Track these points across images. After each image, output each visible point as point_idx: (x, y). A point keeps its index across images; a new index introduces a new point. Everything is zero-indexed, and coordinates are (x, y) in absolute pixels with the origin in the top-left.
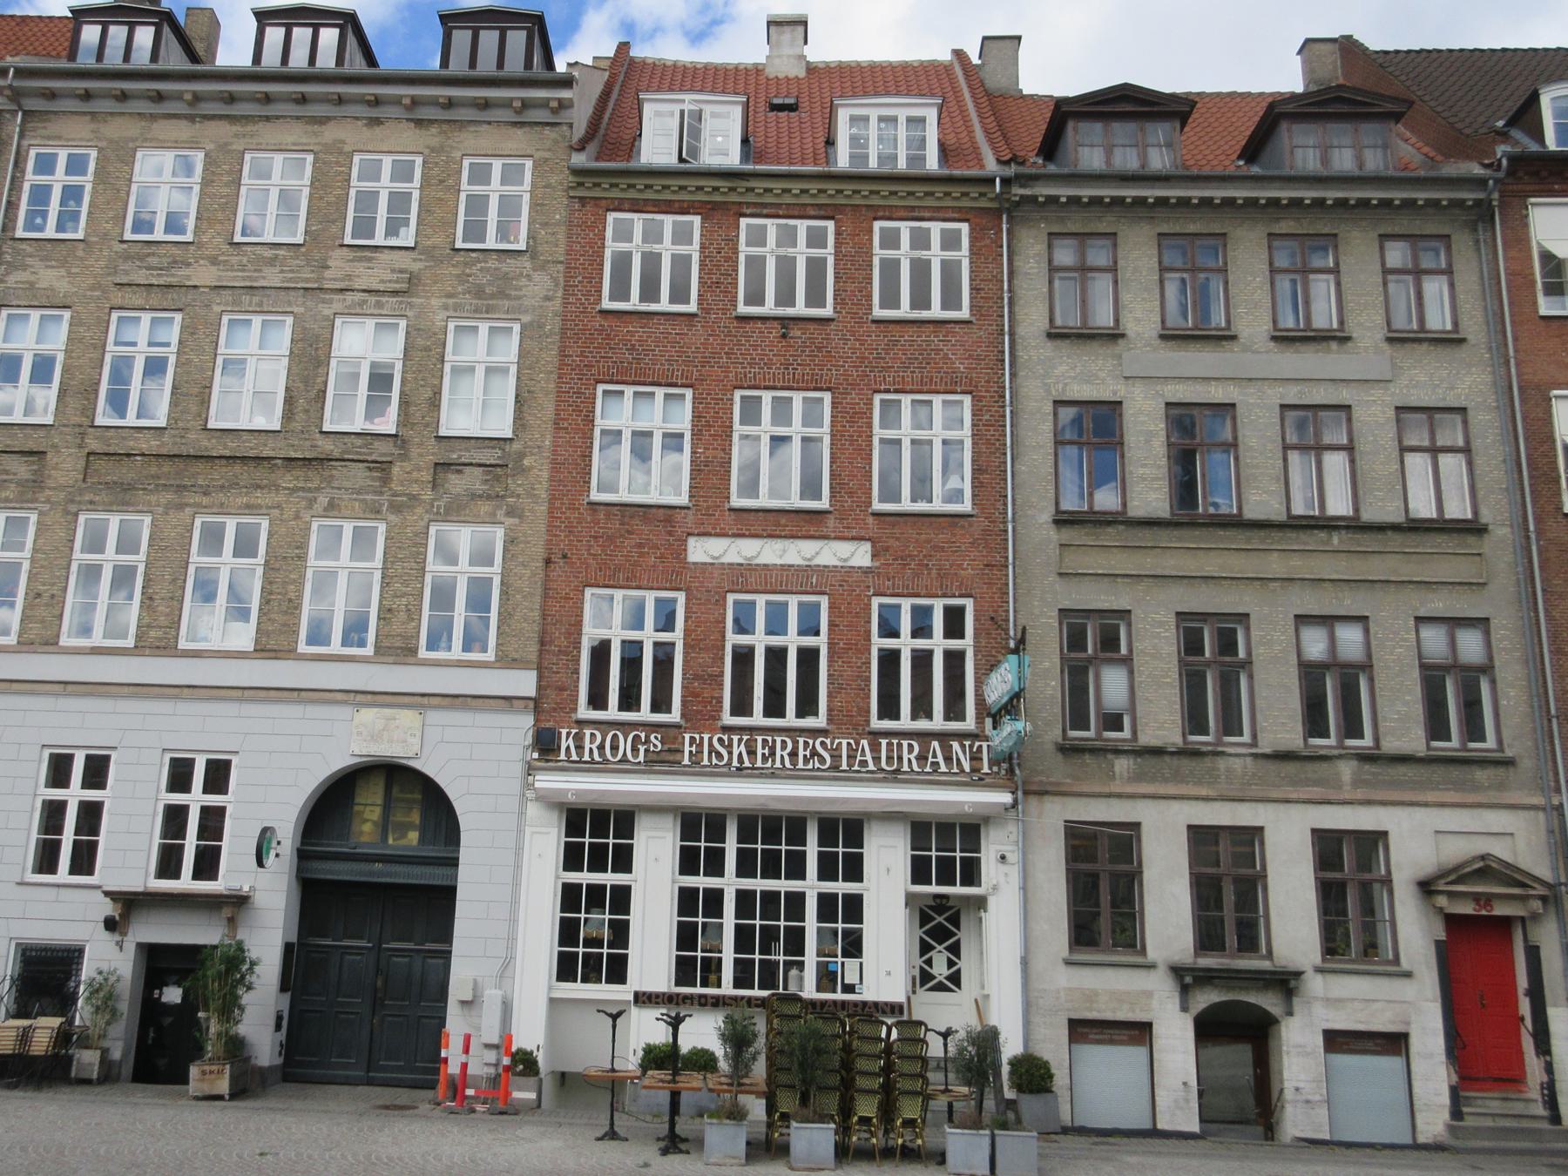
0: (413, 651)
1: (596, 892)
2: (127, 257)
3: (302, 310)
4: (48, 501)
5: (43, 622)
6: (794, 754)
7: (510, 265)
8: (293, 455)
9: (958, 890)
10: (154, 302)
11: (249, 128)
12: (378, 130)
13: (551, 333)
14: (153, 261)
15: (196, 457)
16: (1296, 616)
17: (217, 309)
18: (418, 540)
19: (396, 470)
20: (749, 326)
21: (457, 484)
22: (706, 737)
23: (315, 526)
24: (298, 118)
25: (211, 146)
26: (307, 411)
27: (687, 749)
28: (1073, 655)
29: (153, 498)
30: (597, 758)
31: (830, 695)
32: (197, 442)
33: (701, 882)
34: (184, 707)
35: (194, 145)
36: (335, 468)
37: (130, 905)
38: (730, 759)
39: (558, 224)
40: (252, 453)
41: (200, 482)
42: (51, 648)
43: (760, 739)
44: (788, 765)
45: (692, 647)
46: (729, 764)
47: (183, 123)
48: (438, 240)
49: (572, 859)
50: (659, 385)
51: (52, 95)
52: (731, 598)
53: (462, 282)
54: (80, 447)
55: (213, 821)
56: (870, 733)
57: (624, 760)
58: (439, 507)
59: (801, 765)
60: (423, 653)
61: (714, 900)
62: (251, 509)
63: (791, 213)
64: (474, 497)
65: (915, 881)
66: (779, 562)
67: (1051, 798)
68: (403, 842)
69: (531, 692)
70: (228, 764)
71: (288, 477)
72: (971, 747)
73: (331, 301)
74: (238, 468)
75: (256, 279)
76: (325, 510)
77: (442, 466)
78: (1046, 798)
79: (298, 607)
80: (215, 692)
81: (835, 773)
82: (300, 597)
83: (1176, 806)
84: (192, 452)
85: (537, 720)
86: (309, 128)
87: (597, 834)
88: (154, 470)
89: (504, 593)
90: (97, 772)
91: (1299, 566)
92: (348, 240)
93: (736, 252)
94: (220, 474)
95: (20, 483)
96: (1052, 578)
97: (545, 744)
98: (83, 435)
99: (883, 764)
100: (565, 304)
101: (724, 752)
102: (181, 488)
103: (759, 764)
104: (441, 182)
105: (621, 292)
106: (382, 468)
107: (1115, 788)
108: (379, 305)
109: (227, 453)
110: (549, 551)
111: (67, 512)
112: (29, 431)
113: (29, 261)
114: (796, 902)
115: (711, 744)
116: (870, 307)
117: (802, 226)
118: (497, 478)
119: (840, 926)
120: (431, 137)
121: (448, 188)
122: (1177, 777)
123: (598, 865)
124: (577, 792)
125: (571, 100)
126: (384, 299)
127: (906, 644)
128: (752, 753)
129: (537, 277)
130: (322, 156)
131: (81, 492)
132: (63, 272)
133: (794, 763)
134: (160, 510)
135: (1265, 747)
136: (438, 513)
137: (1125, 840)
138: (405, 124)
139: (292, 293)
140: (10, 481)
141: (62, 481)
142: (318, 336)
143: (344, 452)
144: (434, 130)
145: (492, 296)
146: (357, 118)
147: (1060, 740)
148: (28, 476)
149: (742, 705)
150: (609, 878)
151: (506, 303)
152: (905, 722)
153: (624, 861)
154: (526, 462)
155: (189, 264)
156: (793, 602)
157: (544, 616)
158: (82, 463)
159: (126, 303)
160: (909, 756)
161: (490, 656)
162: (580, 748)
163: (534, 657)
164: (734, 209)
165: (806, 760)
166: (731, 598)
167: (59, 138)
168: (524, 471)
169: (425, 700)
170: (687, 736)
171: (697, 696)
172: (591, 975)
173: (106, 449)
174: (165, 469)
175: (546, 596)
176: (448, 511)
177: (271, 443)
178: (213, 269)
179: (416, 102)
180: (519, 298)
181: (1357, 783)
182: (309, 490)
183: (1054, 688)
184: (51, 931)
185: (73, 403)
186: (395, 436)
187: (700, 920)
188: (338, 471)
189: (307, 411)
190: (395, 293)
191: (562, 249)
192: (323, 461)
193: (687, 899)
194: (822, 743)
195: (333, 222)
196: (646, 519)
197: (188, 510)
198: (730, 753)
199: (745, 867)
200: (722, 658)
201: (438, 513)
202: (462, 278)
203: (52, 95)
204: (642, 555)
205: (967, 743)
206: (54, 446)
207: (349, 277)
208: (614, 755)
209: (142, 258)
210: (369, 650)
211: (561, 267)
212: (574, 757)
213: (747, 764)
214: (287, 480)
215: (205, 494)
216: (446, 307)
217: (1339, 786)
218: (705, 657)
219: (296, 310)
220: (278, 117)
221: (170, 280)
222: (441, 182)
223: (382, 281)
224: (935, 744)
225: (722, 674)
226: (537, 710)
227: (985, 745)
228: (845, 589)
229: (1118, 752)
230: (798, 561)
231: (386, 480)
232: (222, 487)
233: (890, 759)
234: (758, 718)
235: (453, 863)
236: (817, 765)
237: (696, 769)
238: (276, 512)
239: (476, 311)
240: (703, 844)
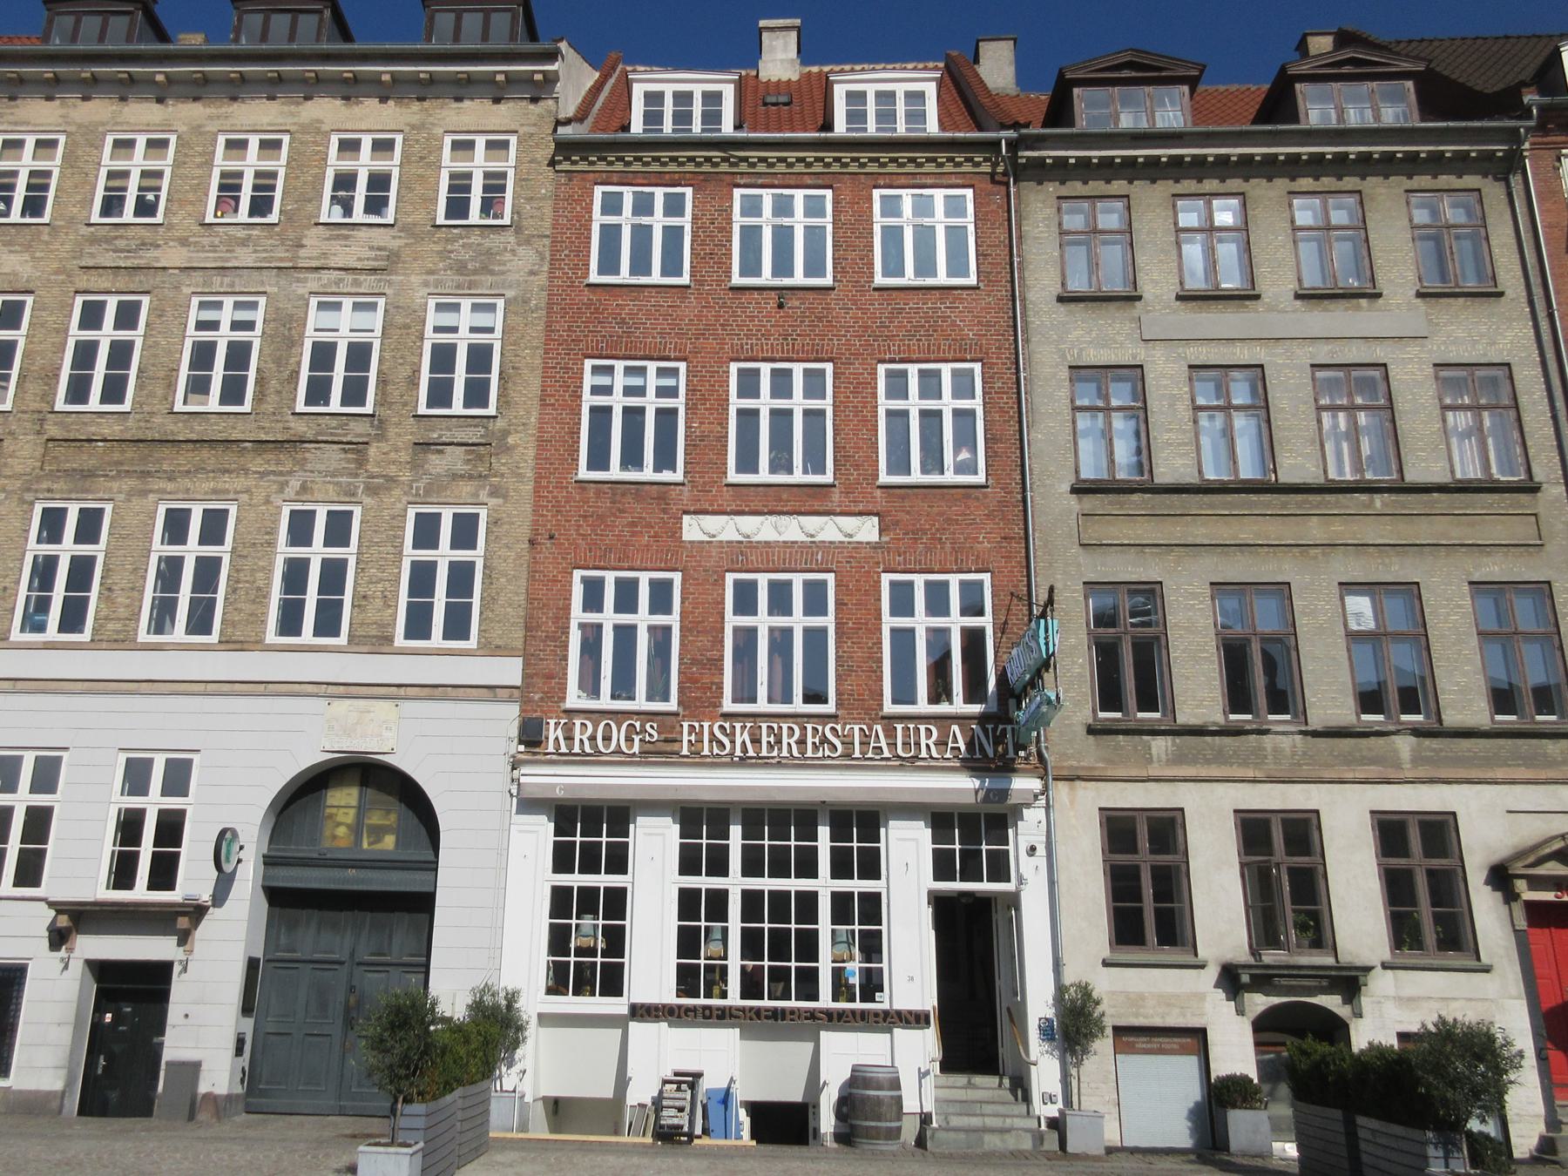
0: (389, 639)
1: (589, 895)
2: (93, 240)
6: (802, 742)
7: (495, 240)
8: (264, 437)
9: (985, 886)
10: (120, 285)
11: (223, 110)
13: (537, 308)
14: (121, 243)
16: (1340, 584)
17: (187, 290)
18: (395, 523)
19: (372, 451)
20: (745, 297)
21: (437, 464)
22: (706, 725)
25: (184, 128)
26: (279, 392)
27: (685, 738)
28: (1101, 630)
29: (115, 485)
30: (588, 750)
31: (838, 677)
32: (162, 426)
33: (704, 882)
36: (308, 450)
37: (76, 919)
38: (734, 748)
39: (543, 198)
41: (165, 467)
43: (764, 726)
44: (795, 753)
45: (690, 630)
46: (732, 754)
48: (419, 216)
49: (562, 861)
50: (651, 359)
52: (730, 578)
53: (443, 259)
54: (39, 433)
55: (171, 828)
56: (883, 718)
57: (618, 751)
58: (418, 489)
59: (809, 754)
60: (400, 641)
61: (718, 901)
62: (217, 493)
63: (787, 182)
64: (455, 477)
65: (938, 876)
66: (781, 539)
67: (1083, 784)
68: (378, 846)
69: (519, 683)
70: (188, 764)
71: (259, 460)
72: (995, 730)
73: (305, 280)
74: (205, 453)
75: (227, 260)
76: (297, 493)
77: (424, 446)
78: (1078, 783)
79: (267, 596)
81: (848, 761)
82: (269, 585)
83: (1220, 788)
84: (157, 436)
85: (522, 711)
86: (286, 108)
87: (589, 832)
88: (116, 456)
89: (487, 576)
91: (1339, 530)
93: (730, 221)
94: (185, 459)
96: (1076, 549)
97: (531, 736)
98: (42, 421)
99: (900, 751)
100: (551, 278)
101: (726, 741)
102: (145, 474)
103: (764, 753)
105: (609, 263)
106: (357, 449)
107: (1154, 771)
108: (356, 283)
109: (194, 437)
110: (535, 532)
111: (24, 502)
114: (808, 902)
115: (712, 733)
116: (872, 275)
117: (799, 195)
118: (480, 458)
119: (857, 927)
121: (429, 165)
122: (1220, 758)
123: (590, 866)
124: (566, 787)
125: (556, 72)
126: (362, 278)
127: (921, 622)
128: (756, 741)
129: (521, 251)
131: (39, 479)
132: (26, 257)
133: (803, 753)
134: (122, 497)
135: (1315, 722)
136: (417, 495)
137: (1167, 829)
139: (265, 272)
141: (19, 469)
142: (291, 316)
143: (318, 434)
145: (475, 272)
147: (1090, 721)
149: (746, 692)
150: (602, 880)
151: (490, 278)
152: (923, 706)
153: (618, 863)
154: (510, 440)
156: (798, 580)
157: (530, 599)
160: (928, 740)
161: (472, 643)
162: (569, 739)
163: (519, 644)
164: (728, 178)
165: (816, 747)
166: (730, 578)
167: (28, 124)
168: (508, 449)
169: (402, 691)
170: (686, 725)
171: (696, 681)
172: (583, 986)
173: (66, 435)
174: (129, 455)
175: (532, 578)
176: (428, 492)
177: (240, 426)
178: (184, 251)
180: (503, 273)
181: (1417, 760)
182: (281, 474)
183: (1081, 666)
185: (33, 388)
186: (373, 416)
187: (703, 924)
188: (312, 454)
189: (279, 392)
190: (374, 270)
191: (548, 223)
193: (688, 902)
194: (833, 729)
195: (310, 201)
196: (638, 497)
197: (152, 497)
198: (733, 742)
199: (751, 867)
200: (722, 641)
201: (417, 495)
202: (444, 255)
204: (634, 534)
205: (990, 727)
206: (11, 433)
207: (324, 255)
208: (607, 747)
209: (108, 240)
210: (342, 640)
211: (547, 242)
212: (564, 749)
213: (751, 753)
214: (257, 464)
215: (170, 480)
216: (426, 284)
217: (1398, 765)
218: (705, 641)
219: (268, 289)
221: (136, 262)
223: (359, 259)
224: (955, 728)
225: (721, 658)
226: (525, 702)
227: (1009, 727)
228: (854, 567)
229: (1155, 733)
230: (802, 538)
231: (361, 462)
232: (188, 472)
233: (906, 744)
234: (762, 705)
235: (432, 867)
236: (827, 753)
237: (697, 759)
238: (245, 497)
239: (458, 287)
240: (704, 841)
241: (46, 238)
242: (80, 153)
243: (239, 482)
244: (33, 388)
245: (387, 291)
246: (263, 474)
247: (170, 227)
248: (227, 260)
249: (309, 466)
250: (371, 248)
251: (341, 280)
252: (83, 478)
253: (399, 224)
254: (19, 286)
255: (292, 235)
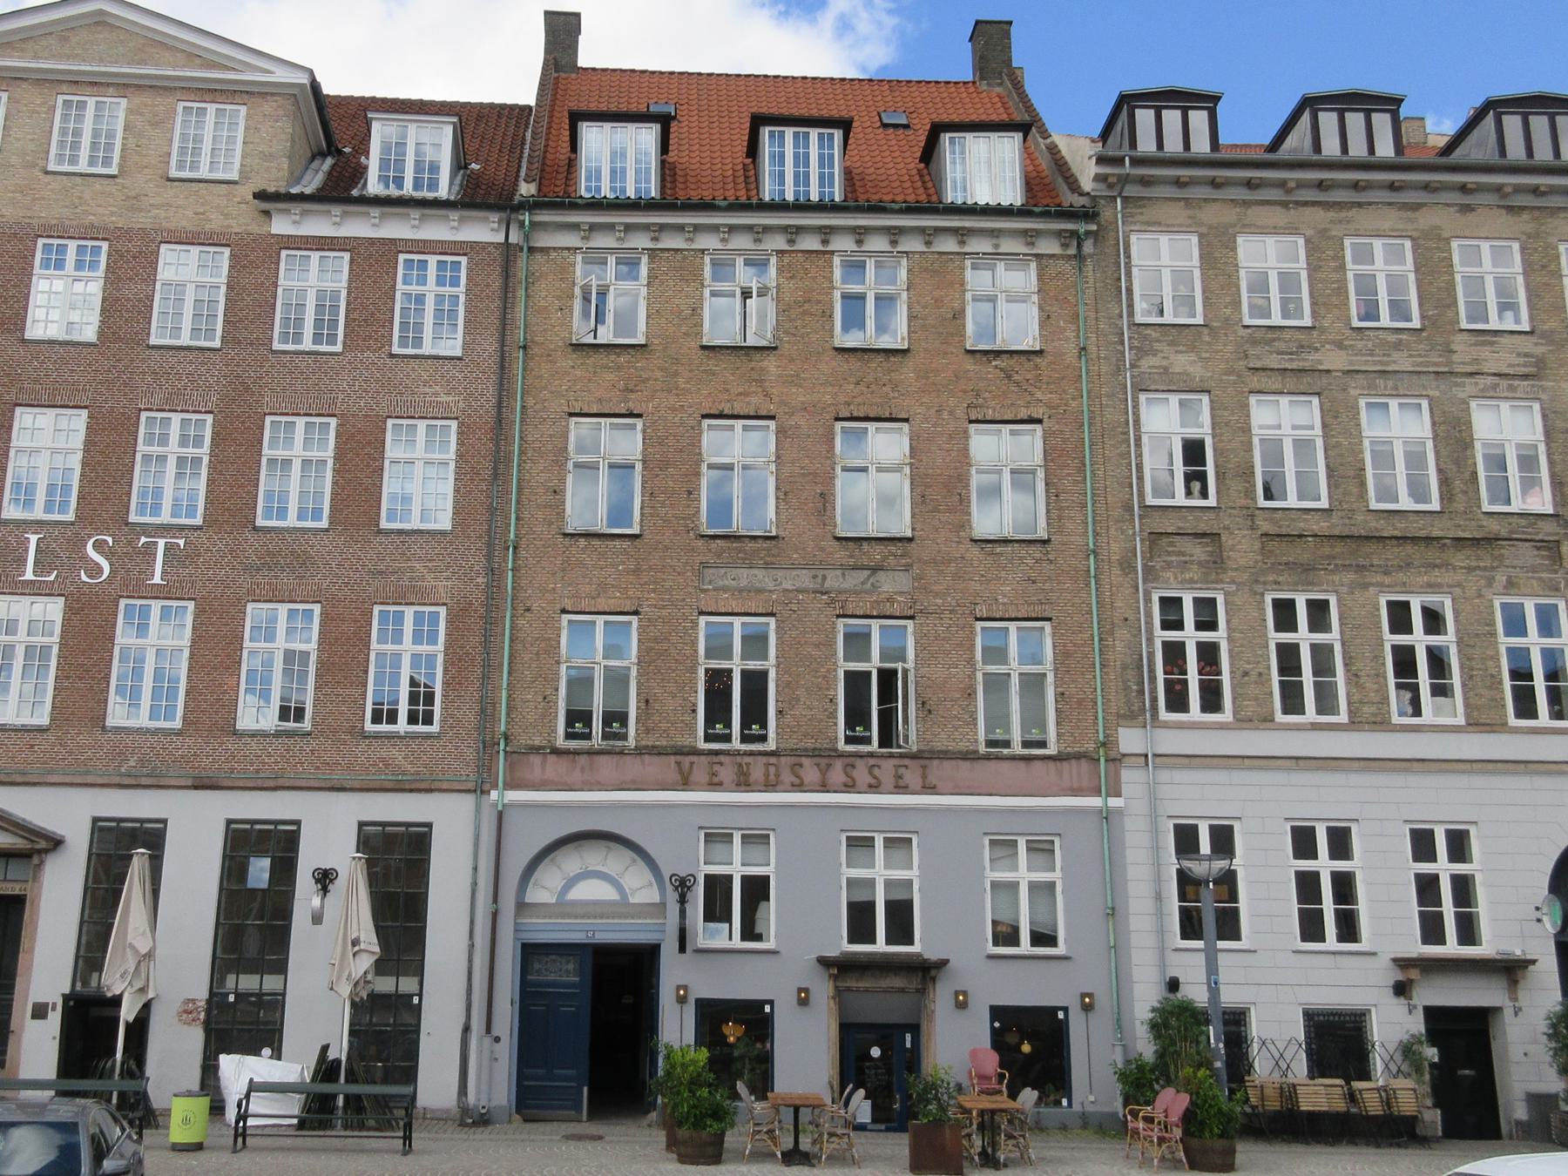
2: (1254, 342)
3: (1437, 393)
4: (1233, 582)
5: (1256, 699)
8: (1461, 534)
11: (1343, 214)
12: (1470, 216)
15: (1367, 538)
23: (1497, 604)
24: (1390, 204)
25: (1310, 233)
29: (1336, 578)
34: (1412, 780)
35: (1292, 230)
36: (1503, 547)
40: (1422, 534)
42: (1268, 725)
47: (1278, 209)
51: (1145, 182)
71: (1460, 556)
73: (1463, 385)
74: (1409, 549)
75: (1387, 363)
76: (1505, 587)
79: (1501, 682)
80: (1444, 765)
82: (1500, 672)
84: (1363, 533)
86: (1403, 214)
88: (1327, 550)
90: (1340, 843)
92: (1464, 325)
94: (1393, 554)
95: (1200, 564)
102: (1361, 569)
104: (1544, 267)
106: (1551, 548)
108: (1511, 388)
112: (1198, 514)
113: (1157, 345)
120: (1524, 223)
126: (1516, 383)
130: (1421, 242)
132: (1193, 357)
134: (1345, 589)
138: (1496, 212)
139: (1423, 377)
140: (1192, 562)
141: (1242, 562)
143: (1512, 532)
144: (1526, 216)
146: (1448, 205)
148: (1204, 557)
155: (1317, 349)
158: (1257, 545)
159: (1263, 387)
178: (1343, 353)
179: (1518, 189)
182: (1485, 569)
184: (1335, 996)
188: (1507, 551)
189: (1465, 492)
190: (1525, 377)
192: (1491, 541)
195: (1448, 306)
203: (1145, 182)
207: (1476, 361)
214: (1460, 559)
219: (1431, 393)
220: (1370, 204)
221: (1301, 365)
222: (1544, 267)
223: (1510, 365)
238: (1457, 590)
241: (1207, 338)
242: (1217, 255)
243: (1447, 577)
244: (1236, 486)
245: (1544, 397)
246: (1470, 569)
247: (1323, 331)
248: (1387, 363)
249: (1507, 562)
250: (1519, 355)
251: (1495, 387)
252: (1306, 573)
253: (1538, 331)
254: (1194, 386)
255: (1440, 340)
